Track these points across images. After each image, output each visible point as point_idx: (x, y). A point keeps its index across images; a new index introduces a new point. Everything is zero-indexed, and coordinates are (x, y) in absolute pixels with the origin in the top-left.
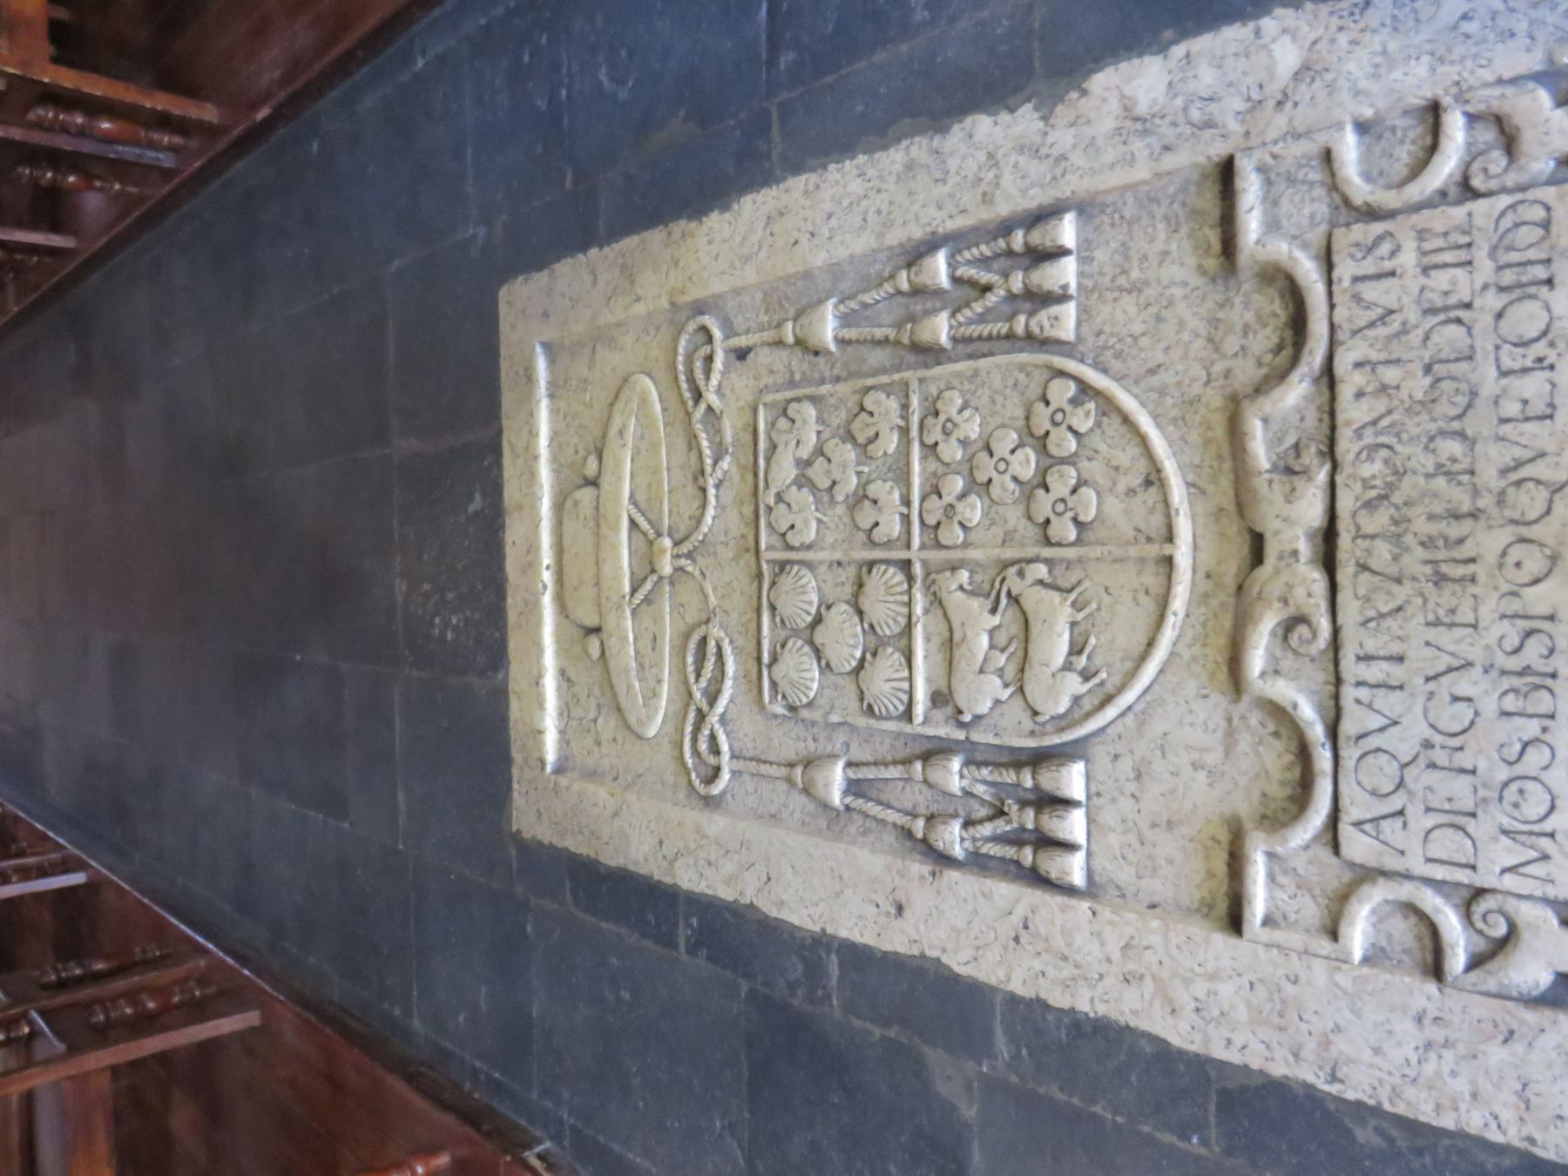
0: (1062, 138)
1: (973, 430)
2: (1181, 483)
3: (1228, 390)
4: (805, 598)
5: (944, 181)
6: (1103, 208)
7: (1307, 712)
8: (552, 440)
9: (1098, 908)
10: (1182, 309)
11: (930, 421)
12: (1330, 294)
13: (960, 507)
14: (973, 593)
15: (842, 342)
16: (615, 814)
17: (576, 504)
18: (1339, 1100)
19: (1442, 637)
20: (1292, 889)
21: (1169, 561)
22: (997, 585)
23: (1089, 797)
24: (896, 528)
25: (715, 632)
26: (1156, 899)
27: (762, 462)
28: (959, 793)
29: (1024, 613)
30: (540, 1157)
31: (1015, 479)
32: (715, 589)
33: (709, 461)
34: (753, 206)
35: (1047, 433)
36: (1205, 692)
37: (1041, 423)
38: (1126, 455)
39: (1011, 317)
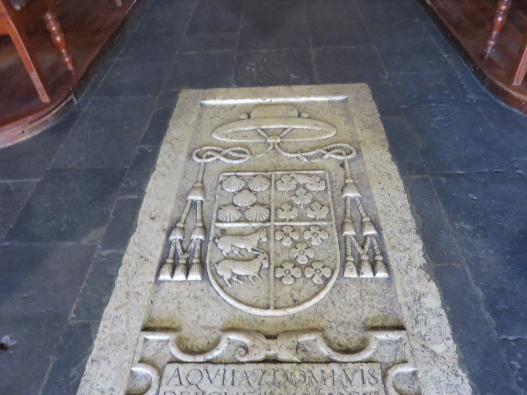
0: (414, 273)
1: (314, 243)
2: (294, 312)
3: (326, 328)
4: (258, 187)
5: (400, 233)
6: (389, 286)
7: (215, 354)
8: (314, 102)
9: (152, 284)
10: (354, 313)
11: (318, 228)
12: (357, 362)
13: (288, 238)
15: (346, 199)
16: (186, 124)
17: (292, 110)
18: (86, 363)
20: (156, 348)
21: (268, 307)
22: (262, 251)
23: (189, 281)
24: (281, 217)
25: (248, 157)
26: (154, 303)
27: (305, 172)
28: (191, 238)
29: (252, 260)
30: (72, 100)
31: (297, 257)
32: (262, 157)
33: (306, 154)
34: (393, 169)
35: (312, 267)
36: (224, 320)
37: (316, 266)
38: (304, 294)
39: (352, 255)
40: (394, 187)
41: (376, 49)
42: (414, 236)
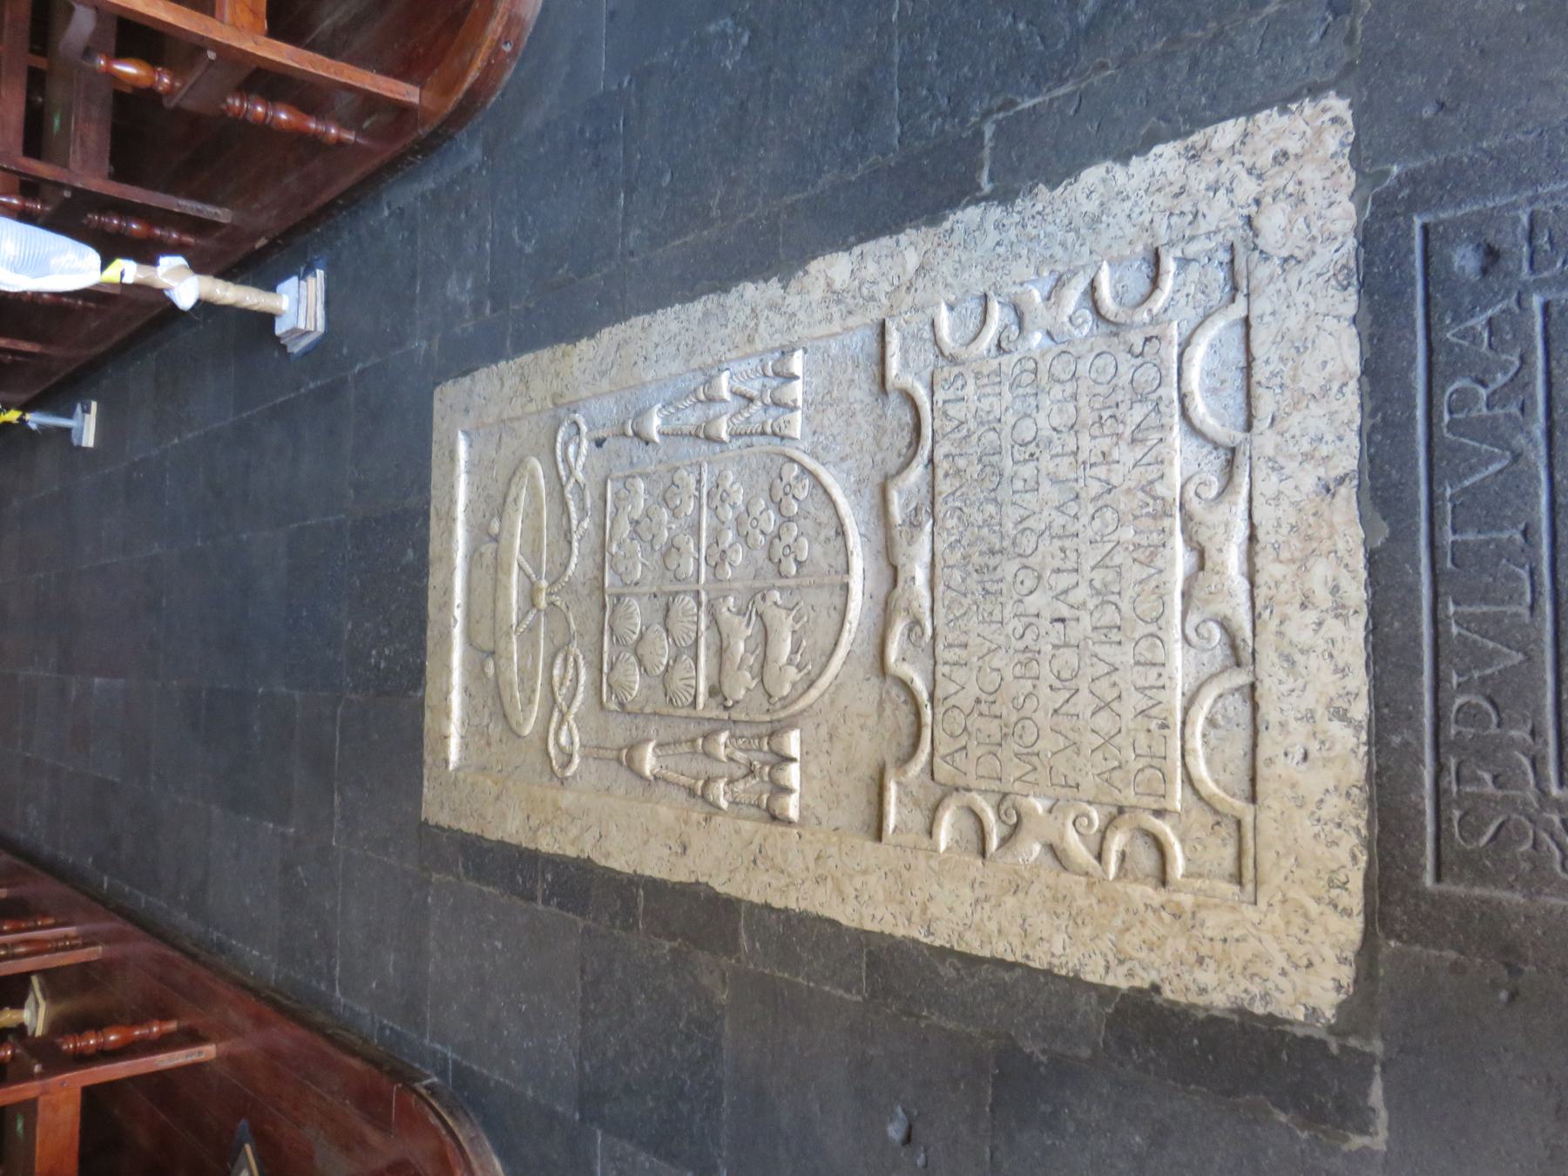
0: (794, 301)
10: (860, 417)
14: (738, 613)
16: (497, 798)
17: (481, 555)
18: (930, 947)
19: (986, 630)
21: (846, 588)
24: (692, 568)
30: (427, 1087)
31: (762, 532)
33: (574, 522)
38: (825, 516)
40: (642, 336)
41: (358, 367)
42: (731, 298)
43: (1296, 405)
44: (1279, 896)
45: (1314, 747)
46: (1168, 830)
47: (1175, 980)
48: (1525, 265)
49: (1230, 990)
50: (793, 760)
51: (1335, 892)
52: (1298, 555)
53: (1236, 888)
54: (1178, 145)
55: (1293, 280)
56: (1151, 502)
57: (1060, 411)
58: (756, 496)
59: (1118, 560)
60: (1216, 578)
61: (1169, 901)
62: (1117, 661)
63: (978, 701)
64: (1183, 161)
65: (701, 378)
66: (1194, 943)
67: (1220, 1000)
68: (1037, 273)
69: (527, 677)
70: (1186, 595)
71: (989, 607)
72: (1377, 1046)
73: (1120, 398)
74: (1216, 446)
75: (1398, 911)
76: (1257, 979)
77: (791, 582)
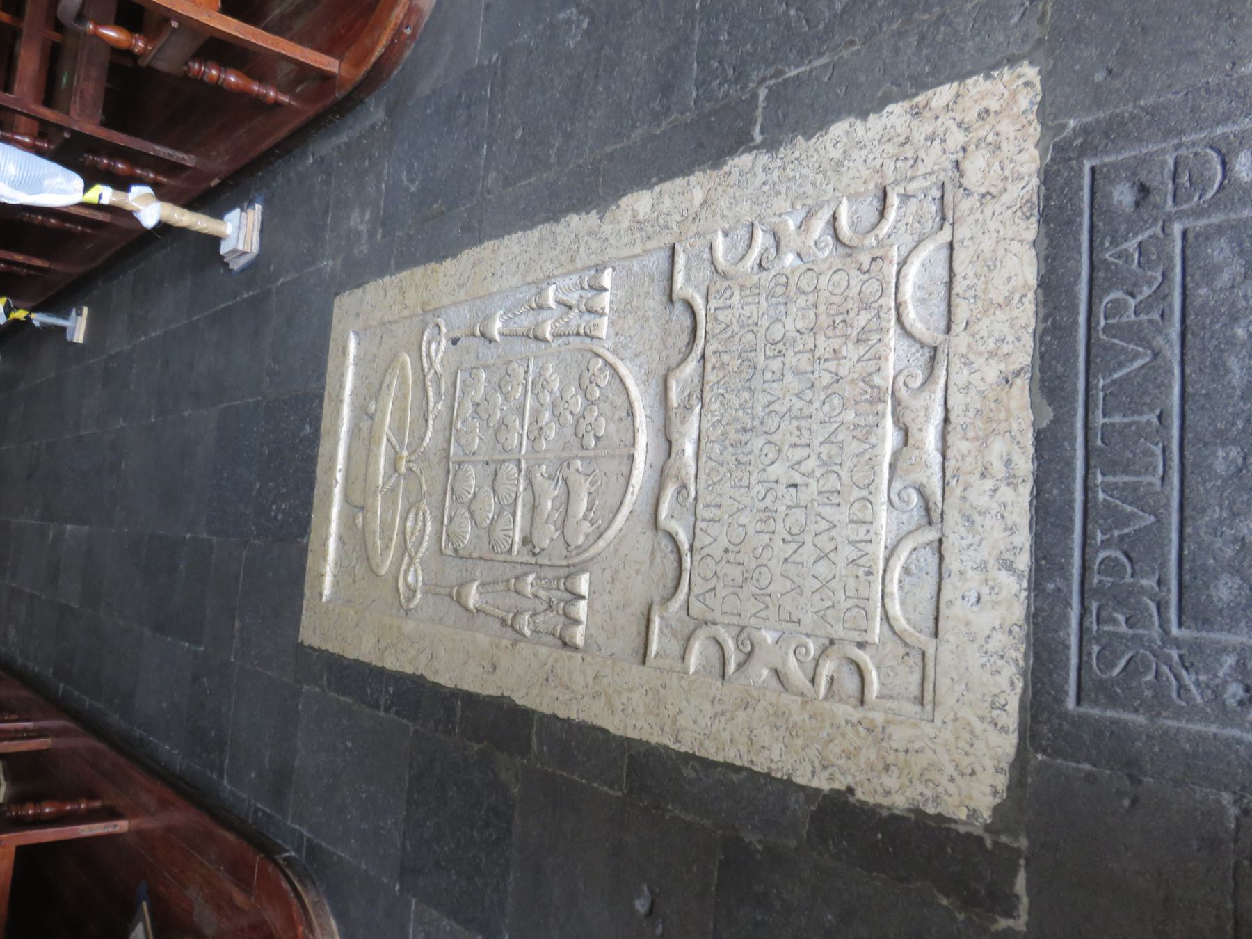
0: (607, 229)
10: (652, 321)
14: (549, 478)
16: (357, 625)
18: (677, 753)
19: (737, 494)
21: (632, 458)
33: (431, 404)
34: (468, 256)
38: (620, 400)
42: (560, 227)
43: (985, 312)
44: (952, 716)
45: (985, 591)
46: (868, 659)
47: (866, 783)
48: (1170, 199)
49: (908, 794)
50: (583, 597)
51: (995, 713)
52: (981, 433)
53: (918, 708)
54: (906, 104)
55: (988, 211)
56: (869, 390)
57: (804, 316)
58: (569, 384)
59: (840, 437)
60: (916, 452)
61: (866, 718)
62: (836, 519)
63: (726, 551)
64: (909, 117)
65: (534, 290)
66: (882, 753)
67: (900, 802)
68: (793, 207)
69: (386, 527)
70: (892, 466)
71: (739, 474)
72: (1023, 843)
73: (850, 306)
74: (922, 345)
75: (1045, 729)
76: (930, 785)
77: (591, 453)
